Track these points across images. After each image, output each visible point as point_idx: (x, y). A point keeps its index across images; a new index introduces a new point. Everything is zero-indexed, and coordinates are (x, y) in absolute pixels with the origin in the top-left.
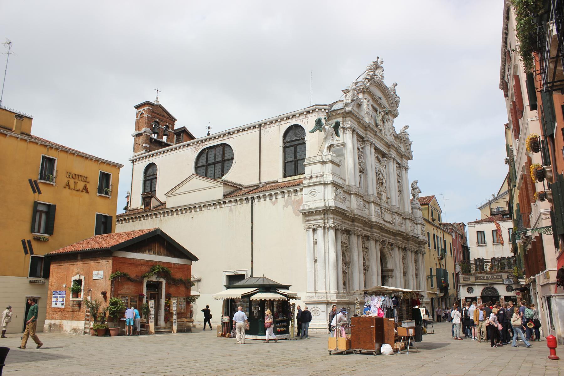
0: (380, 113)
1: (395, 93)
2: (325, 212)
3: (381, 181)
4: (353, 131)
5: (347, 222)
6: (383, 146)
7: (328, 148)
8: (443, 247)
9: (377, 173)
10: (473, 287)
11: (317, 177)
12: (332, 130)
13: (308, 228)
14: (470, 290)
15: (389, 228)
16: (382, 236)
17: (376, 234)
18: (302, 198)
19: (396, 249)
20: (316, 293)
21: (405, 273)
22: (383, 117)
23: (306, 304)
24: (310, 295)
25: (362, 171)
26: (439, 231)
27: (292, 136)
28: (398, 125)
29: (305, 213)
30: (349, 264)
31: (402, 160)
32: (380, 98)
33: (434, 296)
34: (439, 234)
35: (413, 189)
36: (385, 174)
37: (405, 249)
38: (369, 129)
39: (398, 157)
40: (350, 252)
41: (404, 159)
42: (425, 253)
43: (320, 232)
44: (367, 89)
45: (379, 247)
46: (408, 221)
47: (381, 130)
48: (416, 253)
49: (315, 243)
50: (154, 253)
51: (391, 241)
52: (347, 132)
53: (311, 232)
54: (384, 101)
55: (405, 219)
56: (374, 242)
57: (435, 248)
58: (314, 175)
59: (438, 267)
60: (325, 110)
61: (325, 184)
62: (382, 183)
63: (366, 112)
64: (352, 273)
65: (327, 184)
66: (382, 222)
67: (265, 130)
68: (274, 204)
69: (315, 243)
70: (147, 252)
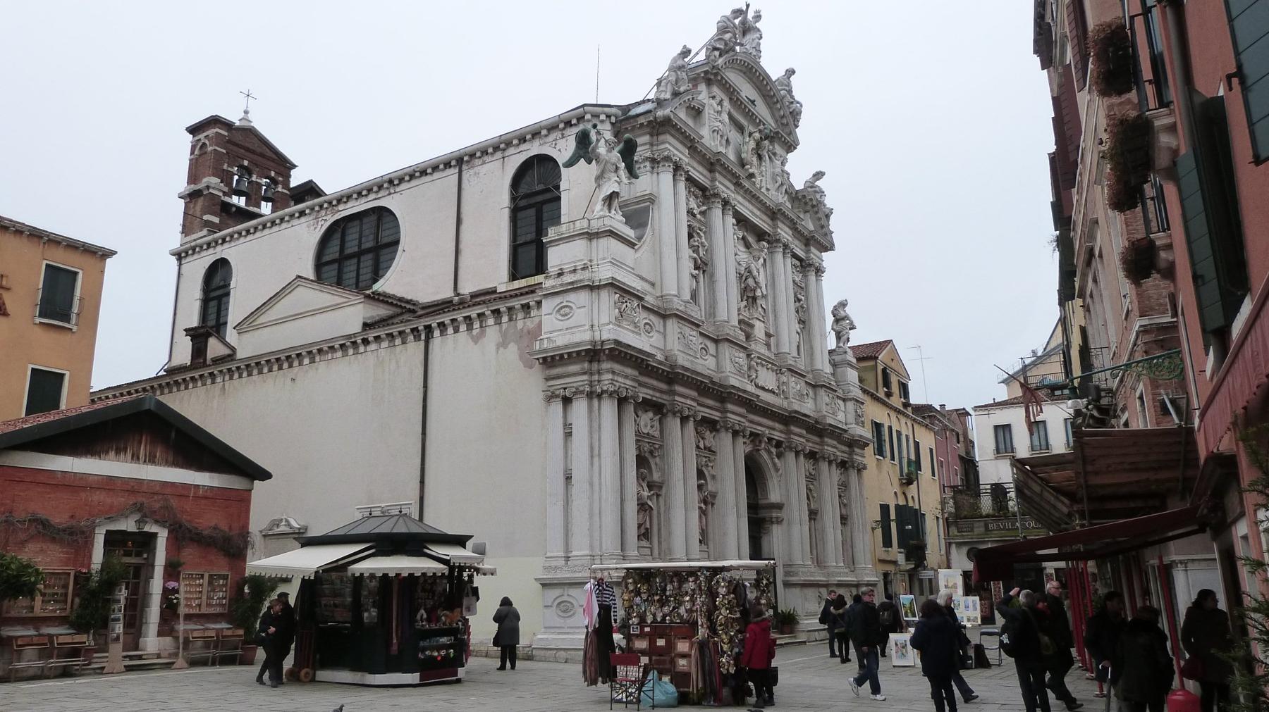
0: (750, 135)
1: (790, 92)
2: (594, 354)
4: (677, 168)
5: (655, 383)
6: (758, 213)
7: (604, 200)
8: (913, 457)
9: (741, 276)
11: (575, 271)
12: (615, 156)
13: (552, 397)
15: (769, 404)
16: (751, 422)
17: (736, 416)
18: (540, 325)
19: (791, 456)
20: (567, 558)
21: (813, 515)
22: (758, 144)
23: (543, 585)
24: (554, 564)
25: (702, 266)
26: (903, 420)
27: (533, 183)
28: (798, 169)
29: (545, 359)
30: (660, 488)
31: (808, 252)
32: (753, 102)
33: (891, 568)
34: (902, 426)
35: (837, 321)
36: (762, 279)
37: (812, 456)
38: (718, 168)
39: (797, 242)
40: (662, 457)
41: (813, 249)
42: (865, 468)
43: (580, 407)
44: (716, 74)
45: (743, 447)
46: (822, 392)
47: (752, 176)
48: (843, 465)
49: (568, 434)
50: (135, 458)
51: (777, 435)
52: (661, 169)
53: (557, 407)
54: (762, 110)
56: (730, 435)
57: (893, 459)
58: (567, 268)
59: (902, 502)
60: (608, 116)
61: (593, 288)
62: (754, 299)
63: (714, 129)
64: (668, 509)
65: (599, 287)
66: (750, 388)
67: (472, 171)
68: (476, 340)
69: (568, 434)
70: (112, 454)
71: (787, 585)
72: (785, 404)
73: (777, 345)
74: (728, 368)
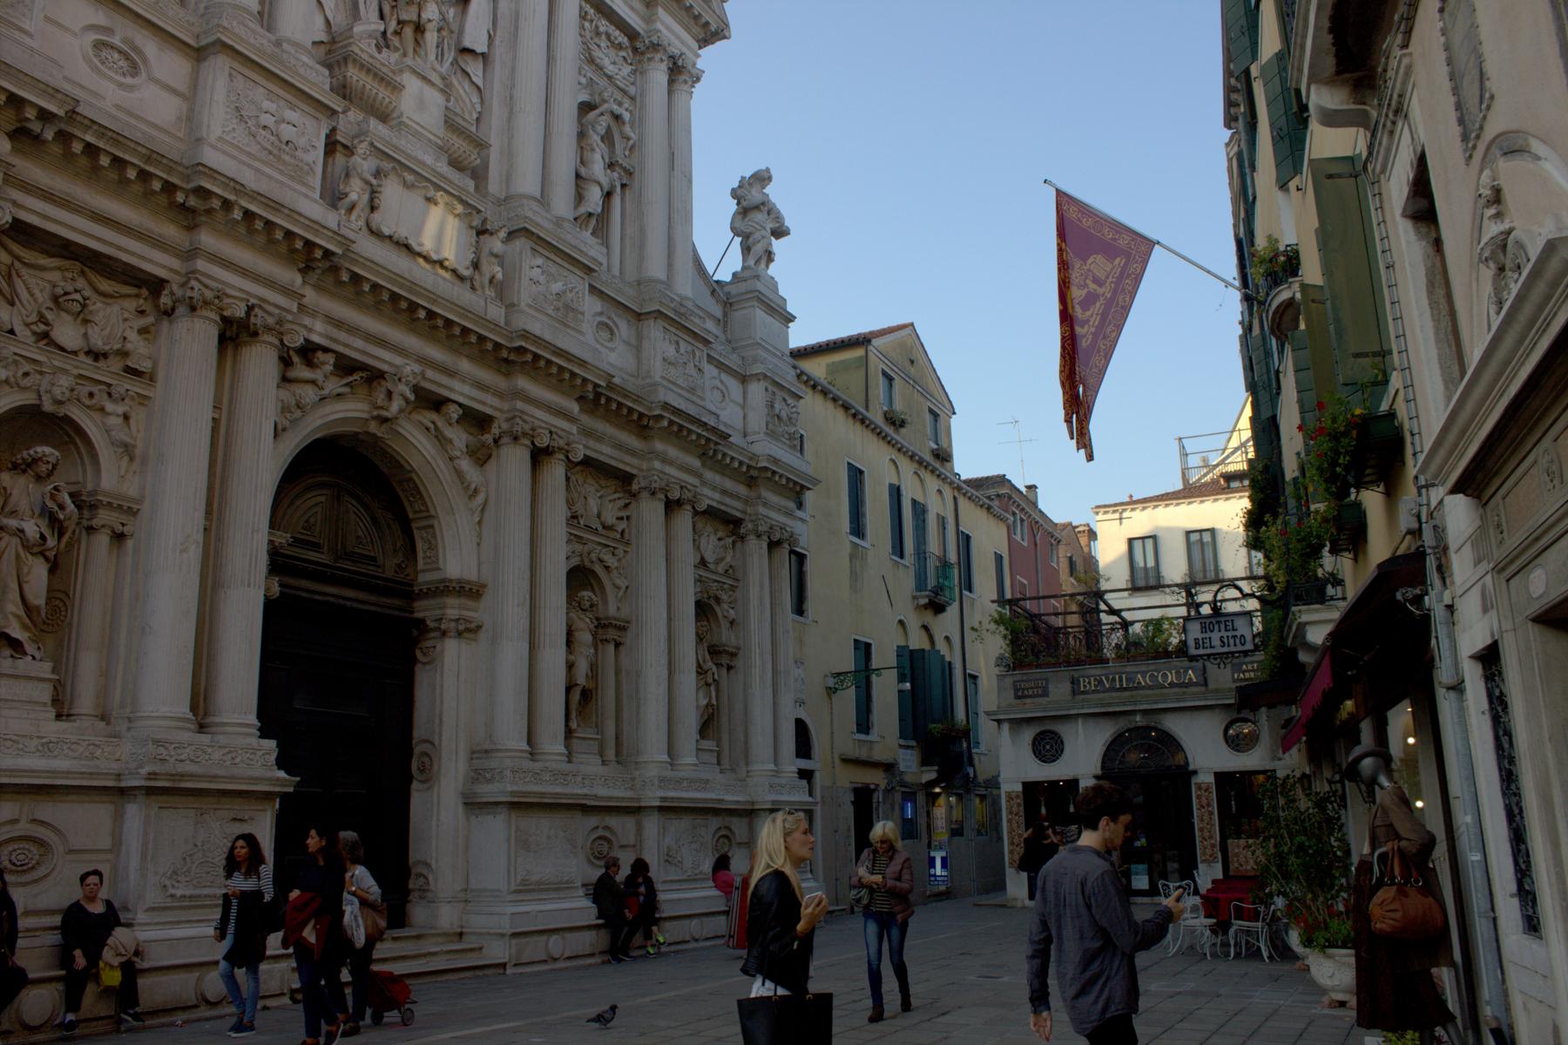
10: (1062, 729)
14: (1048, 746)
15: (413, 286)
31: (649, 20)
33: (876, 778)
46: (655, 332)
51: (461, 392)
55: (639, 316)
57: (899, 550)
59: (917, 641)
62: (419, 29)
71: (474, 805)
72: (496, 312)
73: (508, 179)
74: (217, 120)
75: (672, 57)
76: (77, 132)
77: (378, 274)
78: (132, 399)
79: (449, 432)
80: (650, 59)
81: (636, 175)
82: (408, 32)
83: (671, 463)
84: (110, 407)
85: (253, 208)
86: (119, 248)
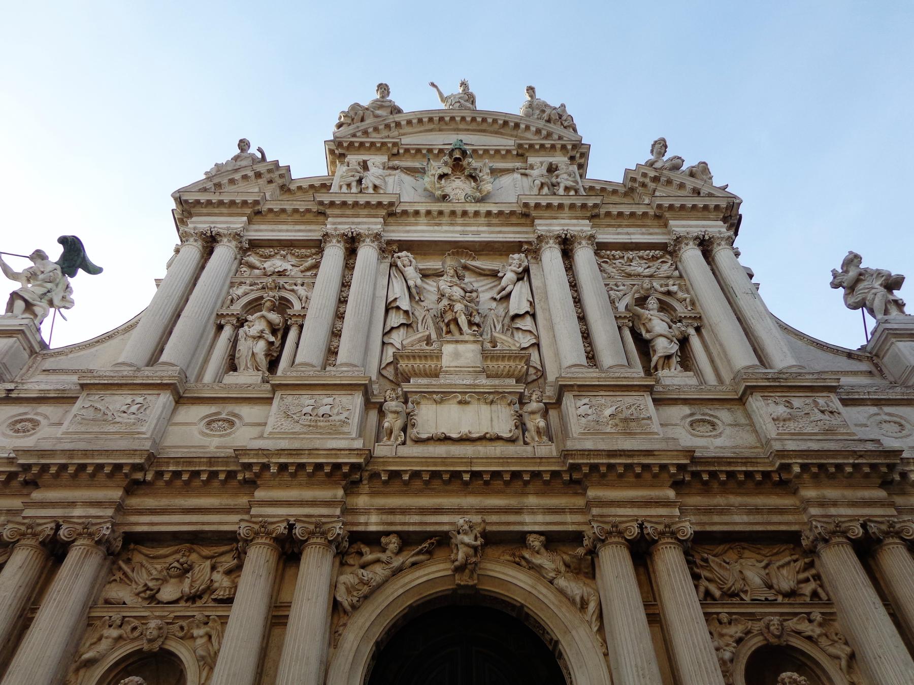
3: (449, 317)
31: (669, 233)
46: (756, 403)
51: (533, 522)
62: (455, 321)
75: (697, 238)
76: (164, 468)
77: (410, 464)
78: (214, 620)
79: (537, 560)
80: (679, 249)
81: (703, 316)
82: (452, 327)
83: (835, 504)
84: (196, 632)
85: (282, 460)
86: (203, 524)
